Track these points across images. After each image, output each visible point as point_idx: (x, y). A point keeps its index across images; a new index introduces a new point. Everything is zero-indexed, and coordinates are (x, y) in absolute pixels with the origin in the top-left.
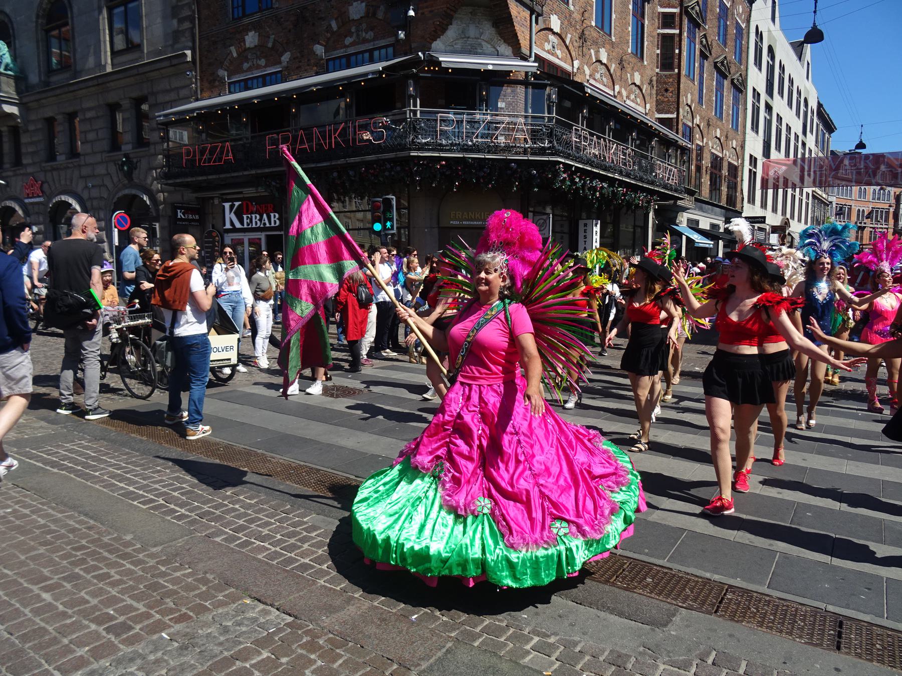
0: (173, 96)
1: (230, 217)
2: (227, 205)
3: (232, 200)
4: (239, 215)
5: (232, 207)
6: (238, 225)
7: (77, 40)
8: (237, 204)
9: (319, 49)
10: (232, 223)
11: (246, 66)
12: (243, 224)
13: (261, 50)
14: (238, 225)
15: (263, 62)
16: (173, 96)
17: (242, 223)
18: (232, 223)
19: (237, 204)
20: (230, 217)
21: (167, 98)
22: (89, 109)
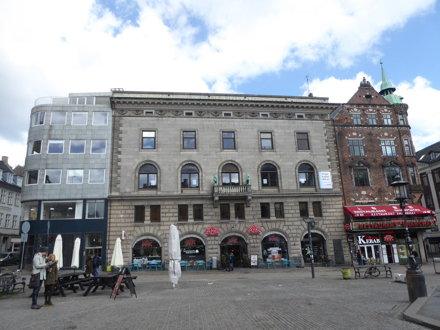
0: (333, 203)
1: (361, 240)
2: (359, 237)
3: (361, 235)
4: (365, 239)
5: (361, 238)
6: (364, 242)
7: (283, 180)
8: (363, 236)
9: (387, 199)
10: (362, 242)
11: (361, 199)
12: (366, 242)
13: (367, 195)
14: (364, 242)
15: (368, 199)
16: (333, 203)
17: (366, 242)
18: (362, 242)
19: (363, 236)
20: (361, 240)
21: (331, 203)
22: (291, 202)
